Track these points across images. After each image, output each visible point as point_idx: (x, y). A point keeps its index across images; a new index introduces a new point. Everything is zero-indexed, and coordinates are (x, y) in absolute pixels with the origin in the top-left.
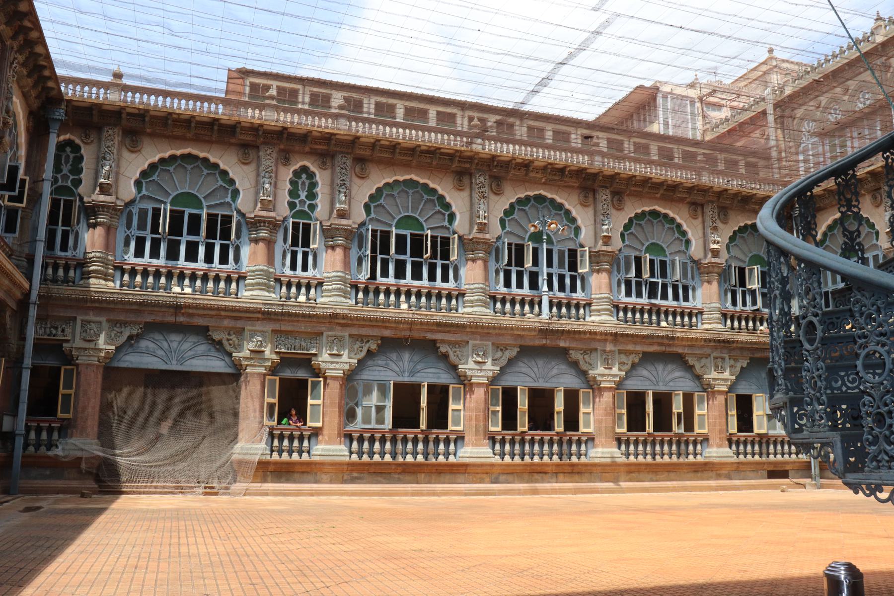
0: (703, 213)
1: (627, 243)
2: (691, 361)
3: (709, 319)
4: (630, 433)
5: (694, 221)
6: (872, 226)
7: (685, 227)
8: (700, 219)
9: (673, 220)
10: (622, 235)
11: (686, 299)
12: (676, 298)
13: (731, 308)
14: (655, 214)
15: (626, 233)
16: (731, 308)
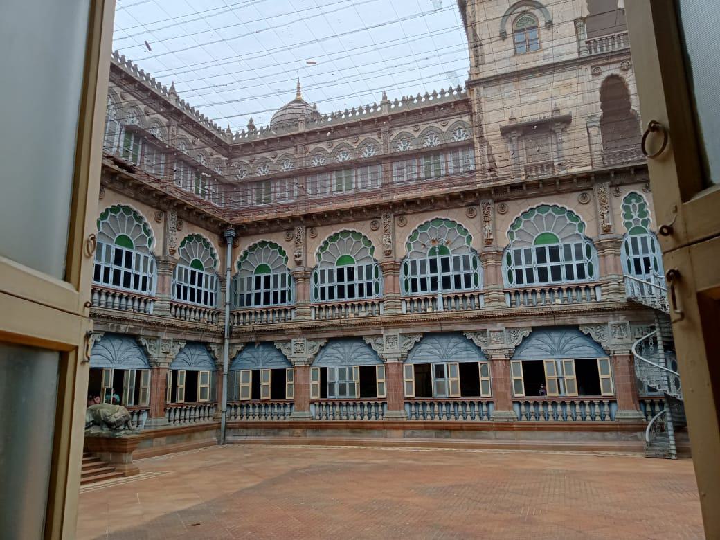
0: (166, 220)
1: (101, 230)
2: (144, 342)
3: (161, 307)
4: (418, 398)
5: (157, 224)
6: (283, 253)
7: (150, 227)
8: (162, 224)
9: (140, 219)
10: (98, 223)
11: (144, 288)
12: (136, 287)
13: (176, 299)
14: (127, 209)
15: (101, 222)
16: (176, 299)
